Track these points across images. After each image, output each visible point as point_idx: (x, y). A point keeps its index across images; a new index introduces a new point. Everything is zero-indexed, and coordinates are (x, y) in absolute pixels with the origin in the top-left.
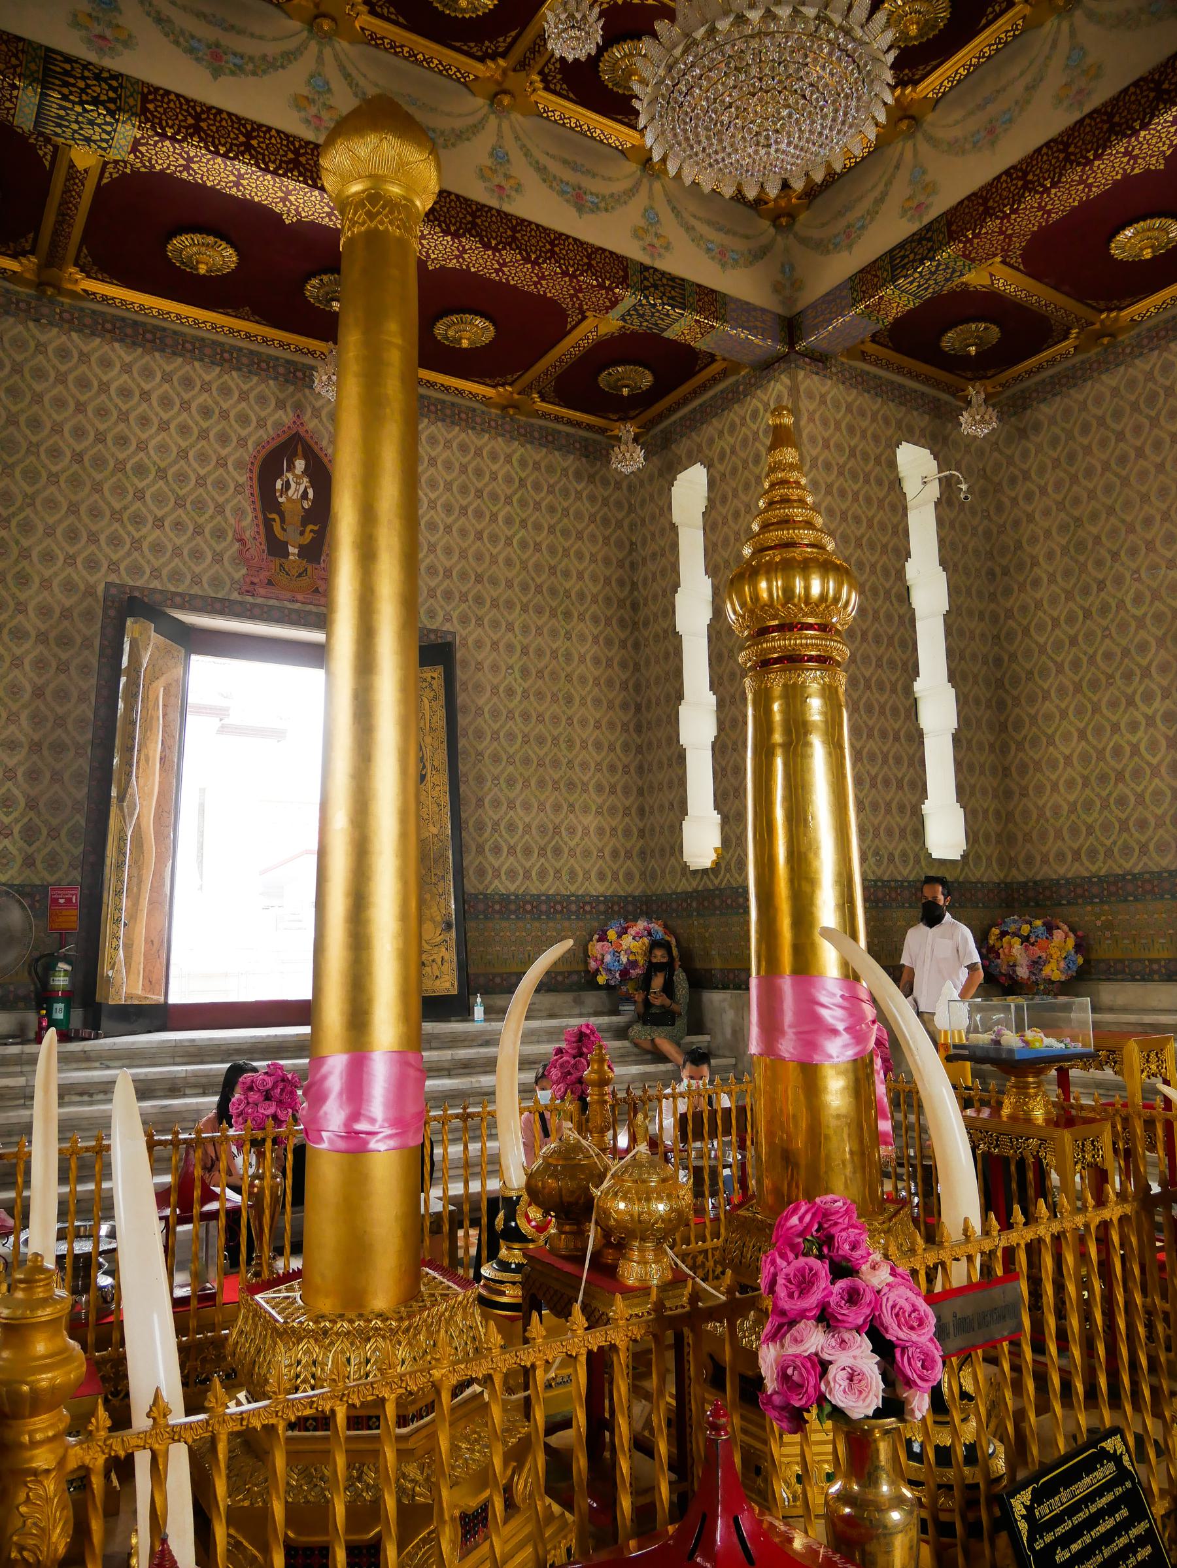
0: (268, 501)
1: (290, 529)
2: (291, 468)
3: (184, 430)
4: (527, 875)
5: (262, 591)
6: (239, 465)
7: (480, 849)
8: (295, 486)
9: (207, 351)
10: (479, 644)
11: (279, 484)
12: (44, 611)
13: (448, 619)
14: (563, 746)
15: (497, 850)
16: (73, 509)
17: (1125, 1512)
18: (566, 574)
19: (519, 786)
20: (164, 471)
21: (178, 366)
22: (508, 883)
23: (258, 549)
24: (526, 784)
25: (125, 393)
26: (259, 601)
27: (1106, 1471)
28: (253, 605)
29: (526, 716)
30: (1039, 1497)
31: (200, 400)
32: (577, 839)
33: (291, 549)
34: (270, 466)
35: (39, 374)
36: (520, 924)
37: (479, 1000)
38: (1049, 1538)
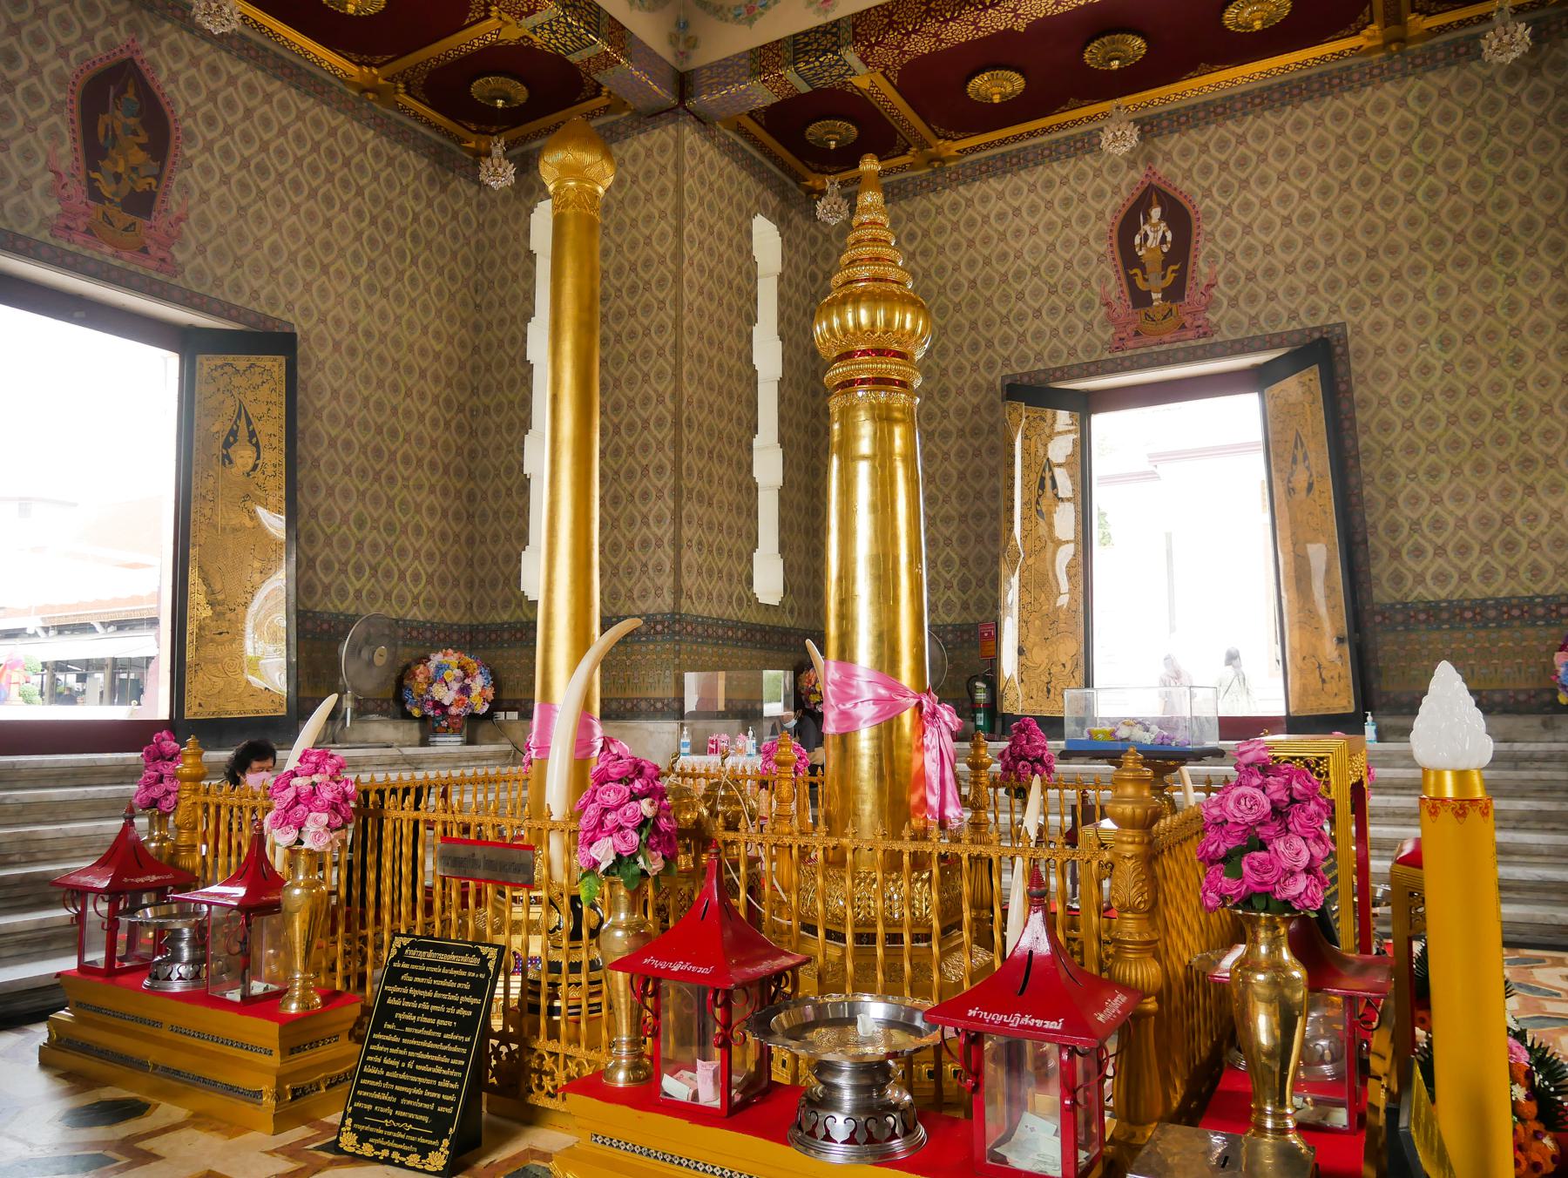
0: (1129, 259)
1: (1151, 277)
2: (1147, 219)
4: (1465, 577)
5: (1130, 344)
6: (1098, 238)
7: (1395, 554)
8: (1155, 233)
9: (1063, 148)
10: (1378, 327)
11: (1137, 240)
12: (961, 412)
13: (1334, 309)
14: (1511, 416)
15: (1418, 552)
16: (973, 326)
17: (467, 986)
19: (1446, 475)
20: (1038, 268)
21: (1041, 173)
22: (1437, 589)
23: (1123, 306)
24: (1457, 471)
25: (1001, 216)
26: (1128, 353)
27: (474, 961)
28: (1123, 359)
29: (1451, 393)
30: (412, 945)
31: (1061, 194)
32: (1541, 527)
33: (1154, 296)
34: (1129, 225)
35: (940, 230)
36: (1458, 635)
37: (1369, 718)
38: (405, 966)
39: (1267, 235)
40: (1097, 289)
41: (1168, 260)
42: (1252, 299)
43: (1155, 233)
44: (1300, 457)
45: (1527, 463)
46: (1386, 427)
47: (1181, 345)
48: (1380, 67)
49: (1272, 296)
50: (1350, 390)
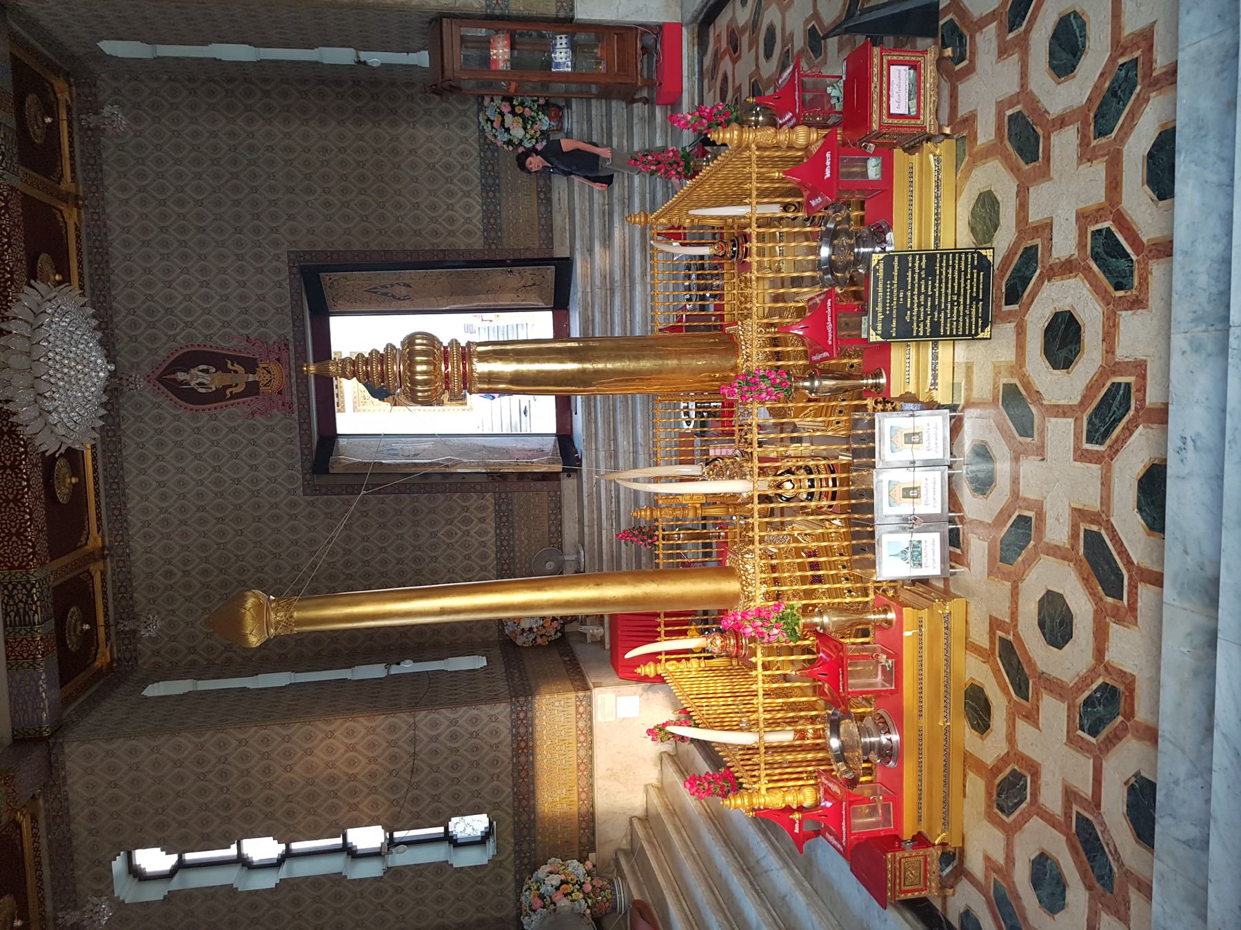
0: (218, 396)
3: (180, 457)
5: (288, 398)
9: (111, 447)
10: (293, 231)
11: (201, 390)
13: (277, 257)
18: (215, 148)
26: (295, 400)
29: (344, 191)
34: (190, 396)
39: (213, 298)
40: (239, 421)
41: (222, 368)
42: (262, 311)
43: (200, 378)
44: (384, 290)
45: (395, 152)
46: (366, 232)
47: (293, 361)
48: (92, 213)
49: (262, 298)
50: (338, 252)
